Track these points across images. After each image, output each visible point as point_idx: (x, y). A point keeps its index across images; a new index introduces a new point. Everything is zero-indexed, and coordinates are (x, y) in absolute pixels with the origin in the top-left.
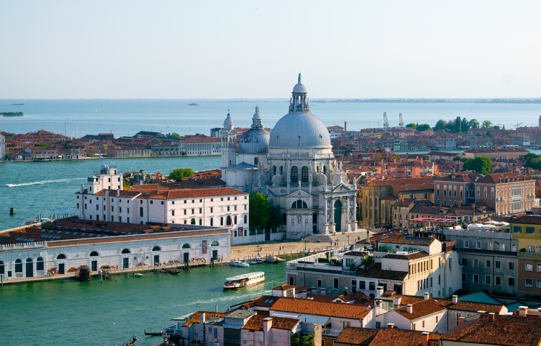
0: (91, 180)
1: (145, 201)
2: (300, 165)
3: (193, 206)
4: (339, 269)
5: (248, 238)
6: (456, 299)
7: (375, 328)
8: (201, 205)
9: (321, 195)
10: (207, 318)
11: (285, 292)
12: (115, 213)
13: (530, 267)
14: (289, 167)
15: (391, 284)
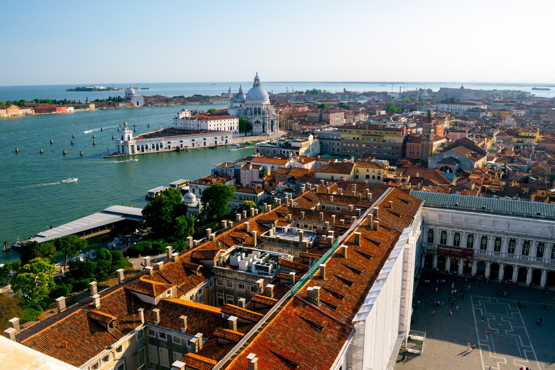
0: (178, 113)
1: (199, 121)
2: (257, 107)
3: (217, 123)
4: (275, 146)
5: (238, 135)
6: (319, 157)
8: (221, 122)
10: (228, 165)
12: (188, 126)
13: (345, 145)
14: (253, 108)
15: (295, 151)
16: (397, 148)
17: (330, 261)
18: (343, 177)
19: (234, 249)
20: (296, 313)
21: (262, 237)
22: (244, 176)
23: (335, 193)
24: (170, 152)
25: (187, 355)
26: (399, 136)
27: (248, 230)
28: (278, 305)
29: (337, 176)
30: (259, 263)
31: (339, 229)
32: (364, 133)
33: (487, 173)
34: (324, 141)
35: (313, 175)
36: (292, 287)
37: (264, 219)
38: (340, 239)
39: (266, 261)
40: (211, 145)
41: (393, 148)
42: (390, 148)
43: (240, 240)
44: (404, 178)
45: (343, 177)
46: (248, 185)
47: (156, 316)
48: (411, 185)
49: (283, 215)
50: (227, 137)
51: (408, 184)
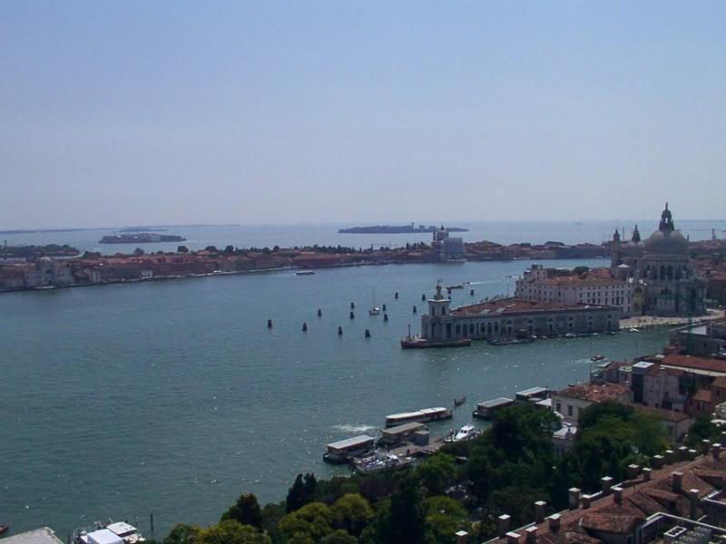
2: (666, 265)
14: (659, 266)
21: (706, 501)
50: (610, 317)
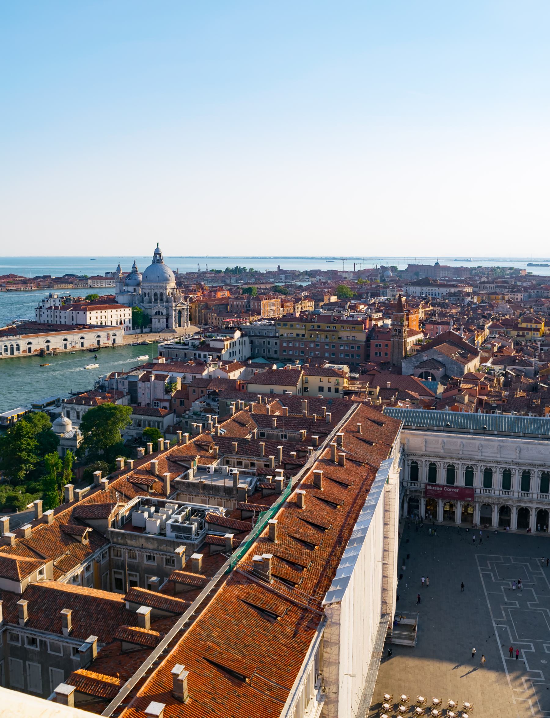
1: (74, 312)
2: (159, 292)
3: (101, 314)
4: (187, 347)
5: (131, 331)
6: (250, 361)
7: (208, 378)
8: (105, 314)
9: (170, 308)
10: (118, 376)
11: (160, 360)
12: (58, 319)
13: (285, 344)
14: (153, 293)
15: (215, 354)
16: (358, 348)
17: (282, 514)
18: (286, 391)
19: (137, 501)
20: (238, 597)
21: (178, 482)
22: (143, 392)
23: (277, 414)
24: (30, 357)
25: (75, 672)
26: (361, 331)
27: (157, 473)
28: (211, 585)
29: (278, 389)
30: (177, 522)
31: (290, 467)
32: (311, 328)
33: (483, 379)
34: (256, 340)
35: (243, 388)
36: (229, 556)
37: (178, 455)
38: (294, 480)
39: (187, 518)
40: (92, 347)
41: (353, 347)
42: (348, 348)
43: (145, 487)
44: (371, 389)
45: (286, 391)
46: (148, 404)
47: (22, 611)
48: (382, 399)
49: (207, 448)
50: (115, 335)
51: (378, 399)
